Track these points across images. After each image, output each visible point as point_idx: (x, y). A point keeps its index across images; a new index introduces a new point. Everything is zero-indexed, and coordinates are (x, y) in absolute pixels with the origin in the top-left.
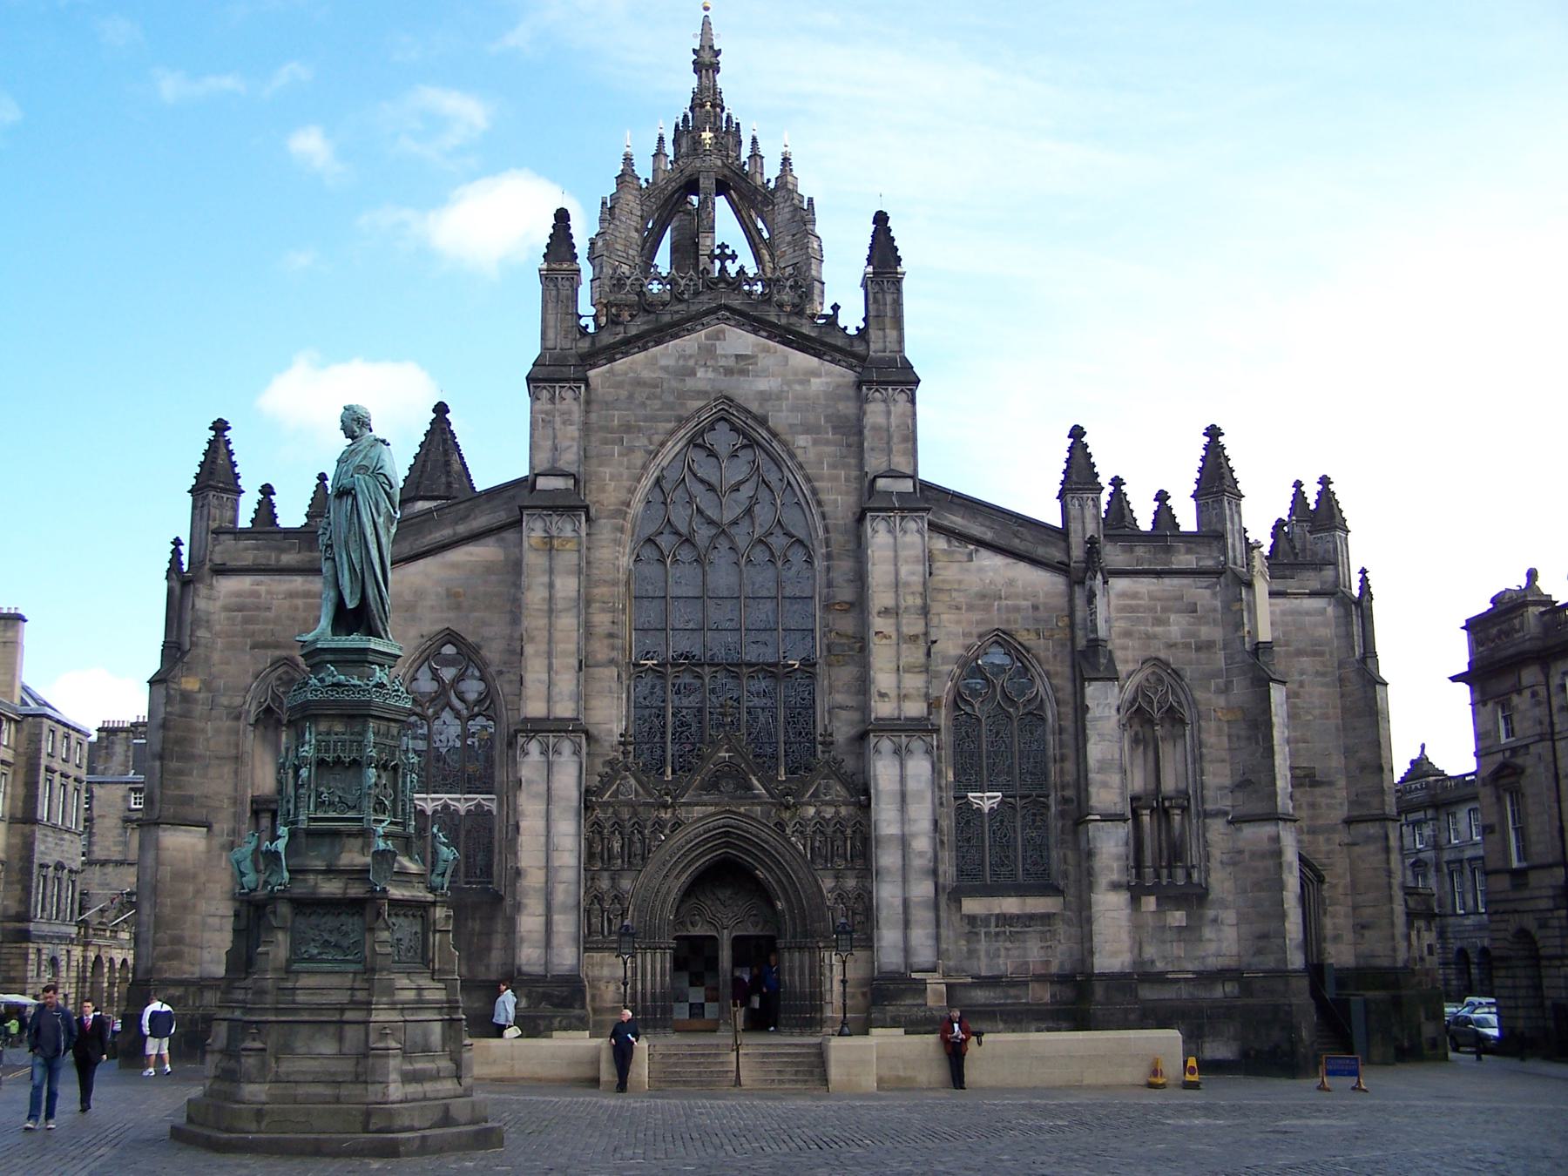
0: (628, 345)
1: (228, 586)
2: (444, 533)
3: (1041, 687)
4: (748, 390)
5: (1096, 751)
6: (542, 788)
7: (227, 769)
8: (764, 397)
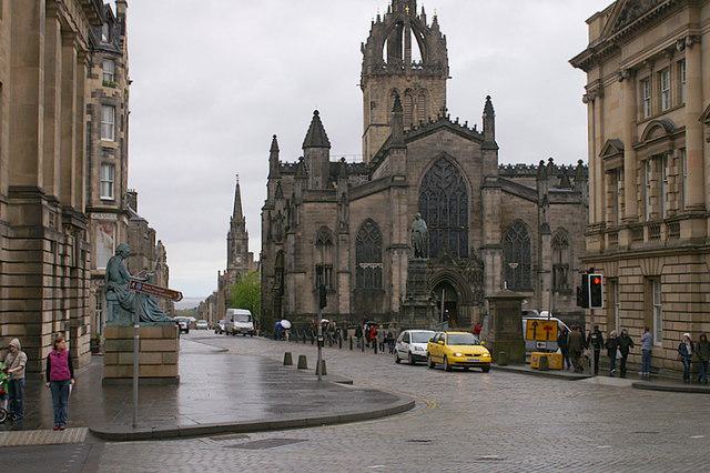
0: (416, 137)
1: (307, 205)
2: (365, 192)
3: (529, 235)
4: (451, 150)
5: (544, 254)
6: (398, 263)
7: (310, 257)
8: (455, 152)
